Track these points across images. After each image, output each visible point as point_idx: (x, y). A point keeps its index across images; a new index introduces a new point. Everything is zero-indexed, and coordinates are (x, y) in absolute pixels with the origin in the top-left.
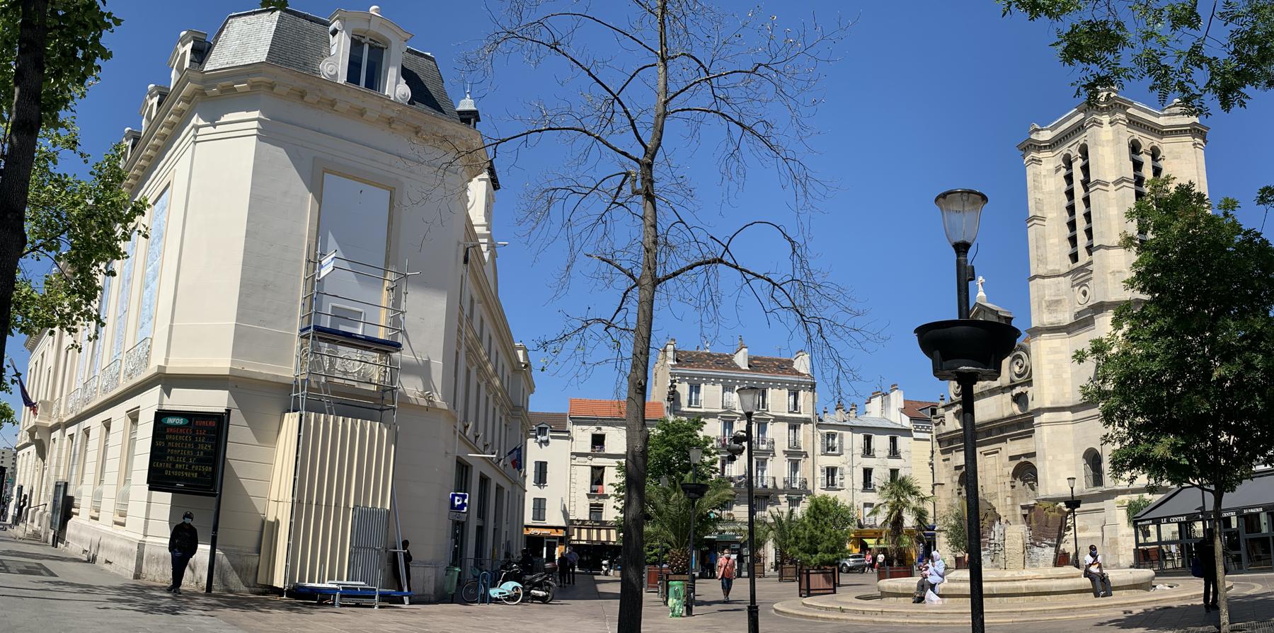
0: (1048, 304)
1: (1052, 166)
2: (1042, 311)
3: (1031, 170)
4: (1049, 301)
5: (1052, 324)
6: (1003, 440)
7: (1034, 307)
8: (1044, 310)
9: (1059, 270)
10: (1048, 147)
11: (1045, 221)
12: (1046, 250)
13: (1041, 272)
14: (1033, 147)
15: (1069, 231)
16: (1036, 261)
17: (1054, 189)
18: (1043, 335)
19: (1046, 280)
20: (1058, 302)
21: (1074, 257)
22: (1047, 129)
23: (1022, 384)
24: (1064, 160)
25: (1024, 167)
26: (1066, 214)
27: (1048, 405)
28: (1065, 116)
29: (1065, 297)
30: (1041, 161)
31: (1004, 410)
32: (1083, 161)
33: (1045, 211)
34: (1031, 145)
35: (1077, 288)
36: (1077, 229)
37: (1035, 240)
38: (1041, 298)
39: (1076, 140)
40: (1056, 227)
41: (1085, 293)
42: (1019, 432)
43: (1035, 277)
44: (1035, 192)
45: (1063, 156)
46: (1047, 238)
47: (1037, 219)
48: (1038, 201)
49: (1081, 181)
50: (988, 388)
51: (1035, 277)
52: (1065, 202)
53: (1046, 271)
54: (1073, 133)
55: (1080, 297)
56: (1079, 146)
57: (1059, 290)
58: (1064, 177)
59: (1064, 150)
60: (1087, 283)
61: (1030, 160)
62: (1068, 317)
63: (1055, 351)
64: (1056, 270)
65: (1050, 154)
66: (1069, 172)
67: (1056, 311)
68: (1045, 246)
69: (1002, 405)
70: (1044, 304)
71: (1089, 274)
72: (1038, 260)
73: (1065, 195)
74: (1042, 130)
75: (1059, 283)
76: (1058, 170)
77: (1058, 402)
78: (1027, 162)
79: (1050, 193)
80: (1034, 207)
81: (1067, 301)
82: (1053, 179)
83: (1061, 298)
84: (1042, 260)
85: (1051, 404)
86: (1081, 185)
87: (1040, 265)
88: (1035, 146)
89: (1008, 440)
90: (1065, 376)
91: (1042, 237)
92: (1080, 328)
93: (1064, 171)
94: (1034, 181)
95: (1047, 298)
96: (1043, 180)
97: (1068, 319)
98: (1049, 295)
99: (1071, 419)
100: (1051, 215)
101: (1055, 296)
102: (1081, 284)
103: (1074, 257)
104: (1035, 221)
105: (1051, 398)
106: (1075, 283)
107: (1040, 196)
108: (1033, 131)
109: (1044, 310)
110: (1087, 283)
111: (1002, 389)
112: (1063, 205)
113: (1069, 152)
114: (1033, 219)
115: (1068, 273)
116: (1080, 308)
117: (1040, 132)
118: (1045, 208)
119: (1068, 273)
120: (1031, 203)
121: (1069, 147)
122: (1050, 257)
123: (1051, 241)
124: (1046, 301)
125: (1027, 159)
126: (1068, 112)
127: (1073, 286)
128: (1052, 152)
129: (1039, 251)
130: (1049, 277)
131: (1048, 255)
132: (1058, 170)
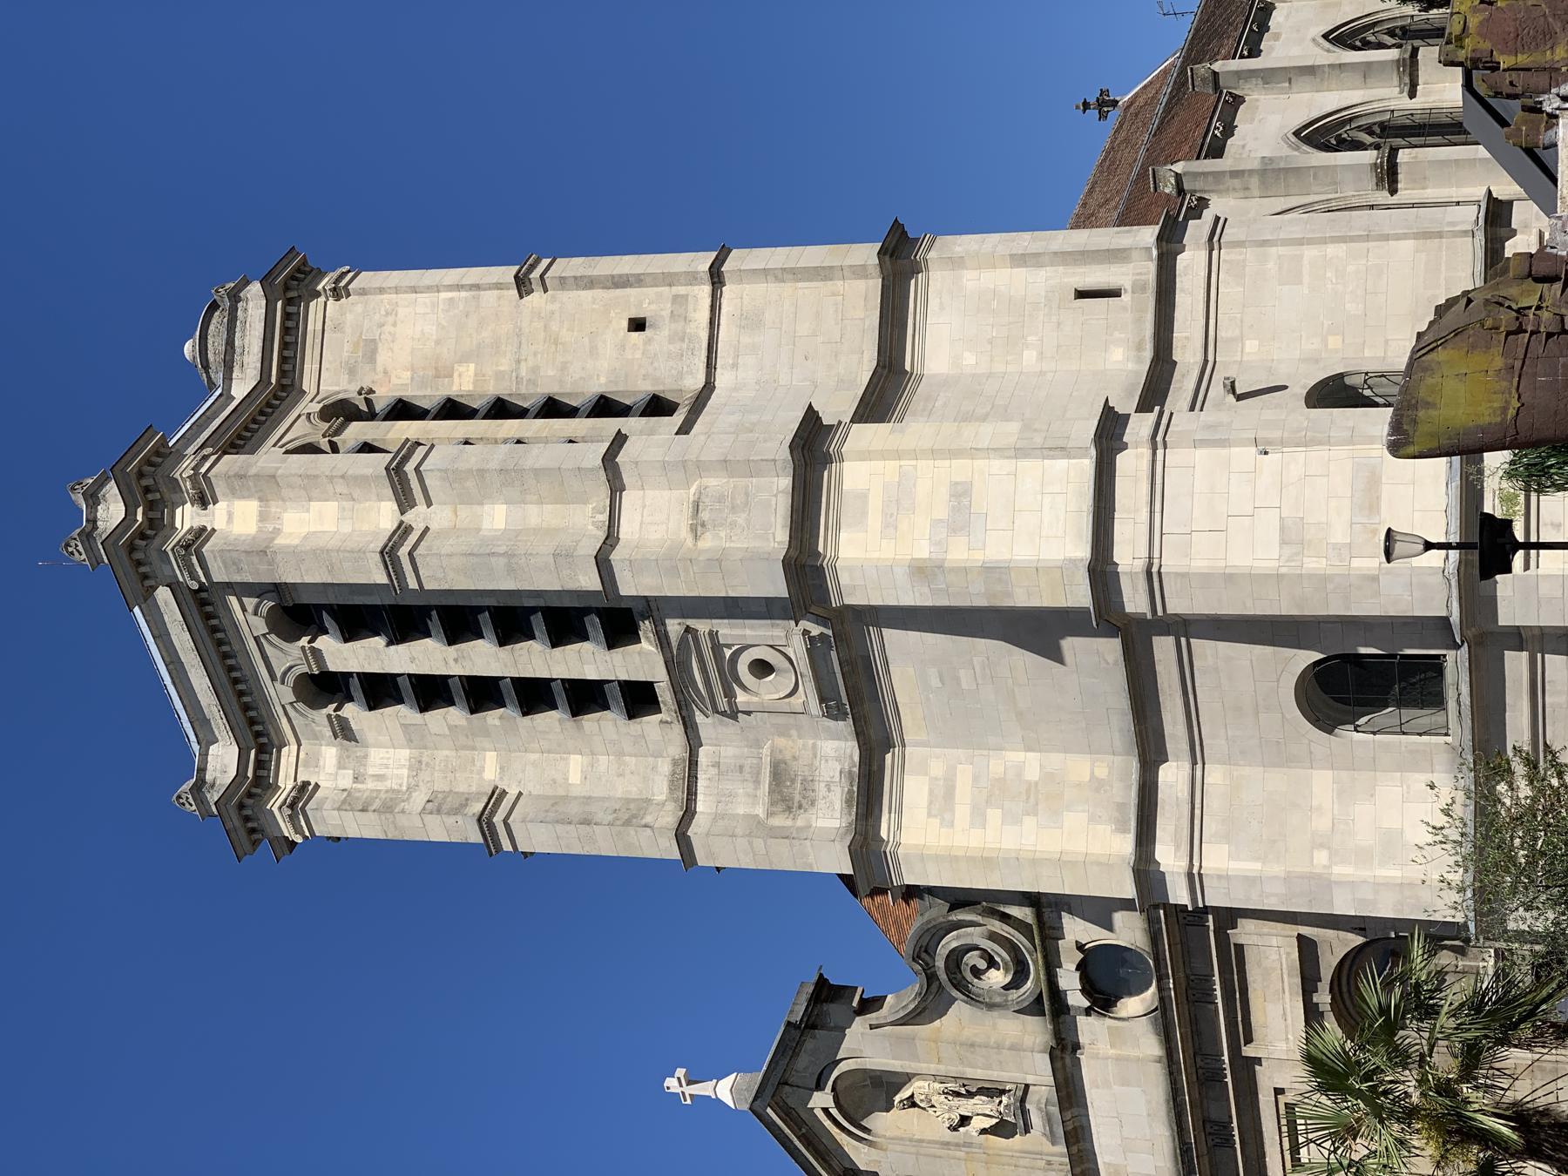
0: (780, 808)
1: (330, 753)
2: (799, 829)
3: (328, 820)
4: (773, 803)
5: (848, 802)
6: (1246, 1069)
7: (783, 858)
8: (800, 823)
9: (675, 763)
10: (265, 757)
11: (504, 793)
12: (603, 799)
13: (669, 817)
14: (250, 802)
15: (553, 713)
16: (632, 831)
17: (404, 754)
18: (884, 834)
19: (701, 807)
20: (779, 774)
21: (639, 699)
22: (204, 755)
23: (1051, 964)
24: (315, 704)
25: (313, 840)
26: (493, 717)
27: (1125, 845)
28: (168, 681)
29: (766, 751)
30: (306, 784)
31: (1134, 1053)
32: (326, 632)
33: (474, 789)
34: (241, 806)
35: (741, 698)
36: (545, 675)
37: (559, 827)
38: (757, 827)
39: (252, 645)
40: (534, 757)
41: (762, 668)
42: (1219, 1001)
43: (682, 838)
44: (403, 812)
45: (300, 706)
46: (561, 792)
47: (493, 813)
48: (435, 805)
49: (390, 643)
50: (1055, 1110)
51: (682, 838)
52: (455, 715)
53: (670, 806)
54: (225, 656)
55: (770, 690)
56: (273, 638)
57: (741, 768)
58: (371, 709)
59: (280, 695)
60: (728, 653)
61: (293, 819)
62: (836, 744)
63: (943, 800)
64: (674, 773)
65: (288, 756)
66: (355, 687)
67: (808, 784)
68: (588, 800)
69: (1118, 1059)
70: (779, 821)
71: (696, 639)
72: (627, 823)
73: (429, 715)
74: (202, 770)
75: (717, 765)
76: (344, 731)
77: (1121, 807)
78: (298, 830)
79: (417, 767)
80: (450, 820)
81: (781, 742)
82: (373, 752)
83: (767, 760)
84: (632, 814)
85: (1125, 831)
86: (402, 648)
87: (648, 819)
88: (250, 795)
89: (1248, 1051)
90: (1032, 773)
91: (557, 809)
92: (875, 697)
93: (353, 712)
94: (362, 810)
95: (760, 811)
96: (370, 785)
97: (842, 744)
98: (751, 802)
99: (1187, 765)
100: (489, 769)
101: (757, 782)
102: (730, 678)
103: (639, 699)
104: (498, 819)
105: (1105, 829)
106: (723, 703)
107: (419, 799)
108: (201, 801)
109: (800, 823)
110: (728, 653)
111: (1063, 1049)
112: (464, 722)
113: (291, 679)
114: (491, 826)
115: (690, 728)
116: (808, 695)
117: (209, 777)
118: (462, 788)
119: (690, 728)
120: (437, 831)
121: (273, 677)
122: (627, 787)
123: (575, 777)
124: (770, 814)
125: (287, 830)
126: (156, 672)
127: (733, 714)
128: (283, 744)
129: (600, 816)
130: (691, 794)
131: (619, 795)
132: (344, 731)
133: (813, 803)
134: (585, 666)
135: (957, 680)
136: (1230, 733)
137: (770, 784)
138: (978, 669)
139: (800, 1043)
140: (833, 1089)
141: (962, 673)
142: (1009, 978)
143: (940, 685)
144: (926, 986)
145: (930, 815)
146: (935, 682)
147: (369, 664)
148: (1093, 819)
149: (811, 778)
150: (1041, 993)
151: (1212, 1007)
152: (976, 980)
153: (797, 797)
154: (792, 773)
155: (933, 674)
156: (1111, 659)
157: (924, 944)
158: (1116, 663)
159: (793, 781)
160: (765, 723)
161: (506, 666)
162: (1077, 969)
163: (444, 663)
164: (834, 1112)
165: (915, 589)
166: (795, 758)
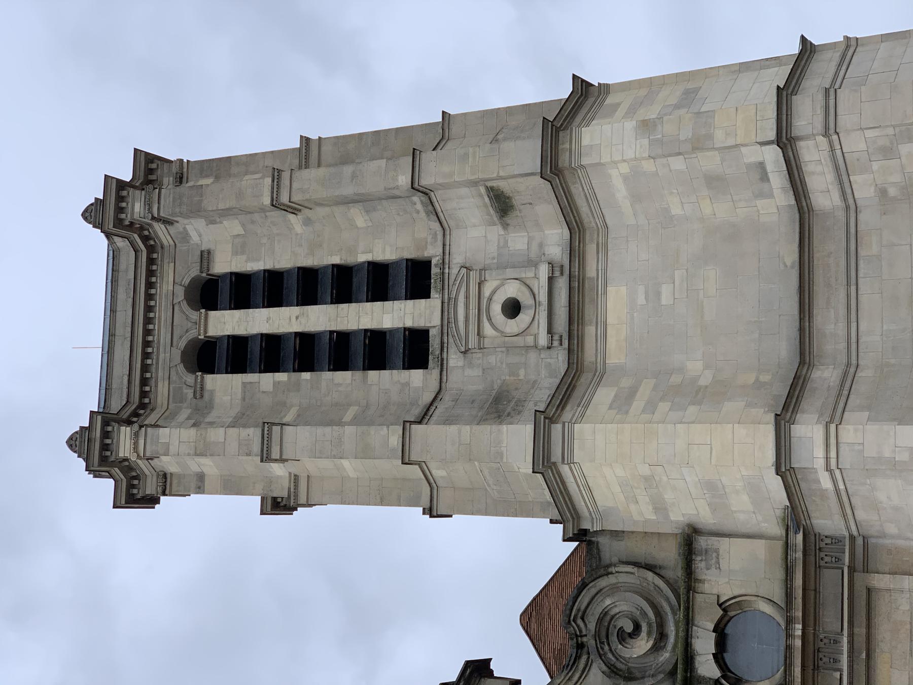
133: (520, 413)
134: (384, 315)
135: (658, 294)
136: (885, 327)
137: (491, 403)
138: (677, 283)
141: (664, 287)
142: (651, 643)
143: (644, 302)
144: (574, 655)
145: (610, 408)
146: (641, 300)
147: (239, 326)
148: (749, 405)
149: (525, 399)
150: (676, 663)
151: (837, 675)
152: (620, 646)
153: (509, 409)
154: (510, 397)
155: (641, 290)
156: (789, 263)
157: (583, 608)
158: (792, 267)
159: (509, 401)
160: (502, 363)
161: (329, 321)
162: (714, 631)
163: (288, 321)
165: (638, 141)
166: (516, 389)
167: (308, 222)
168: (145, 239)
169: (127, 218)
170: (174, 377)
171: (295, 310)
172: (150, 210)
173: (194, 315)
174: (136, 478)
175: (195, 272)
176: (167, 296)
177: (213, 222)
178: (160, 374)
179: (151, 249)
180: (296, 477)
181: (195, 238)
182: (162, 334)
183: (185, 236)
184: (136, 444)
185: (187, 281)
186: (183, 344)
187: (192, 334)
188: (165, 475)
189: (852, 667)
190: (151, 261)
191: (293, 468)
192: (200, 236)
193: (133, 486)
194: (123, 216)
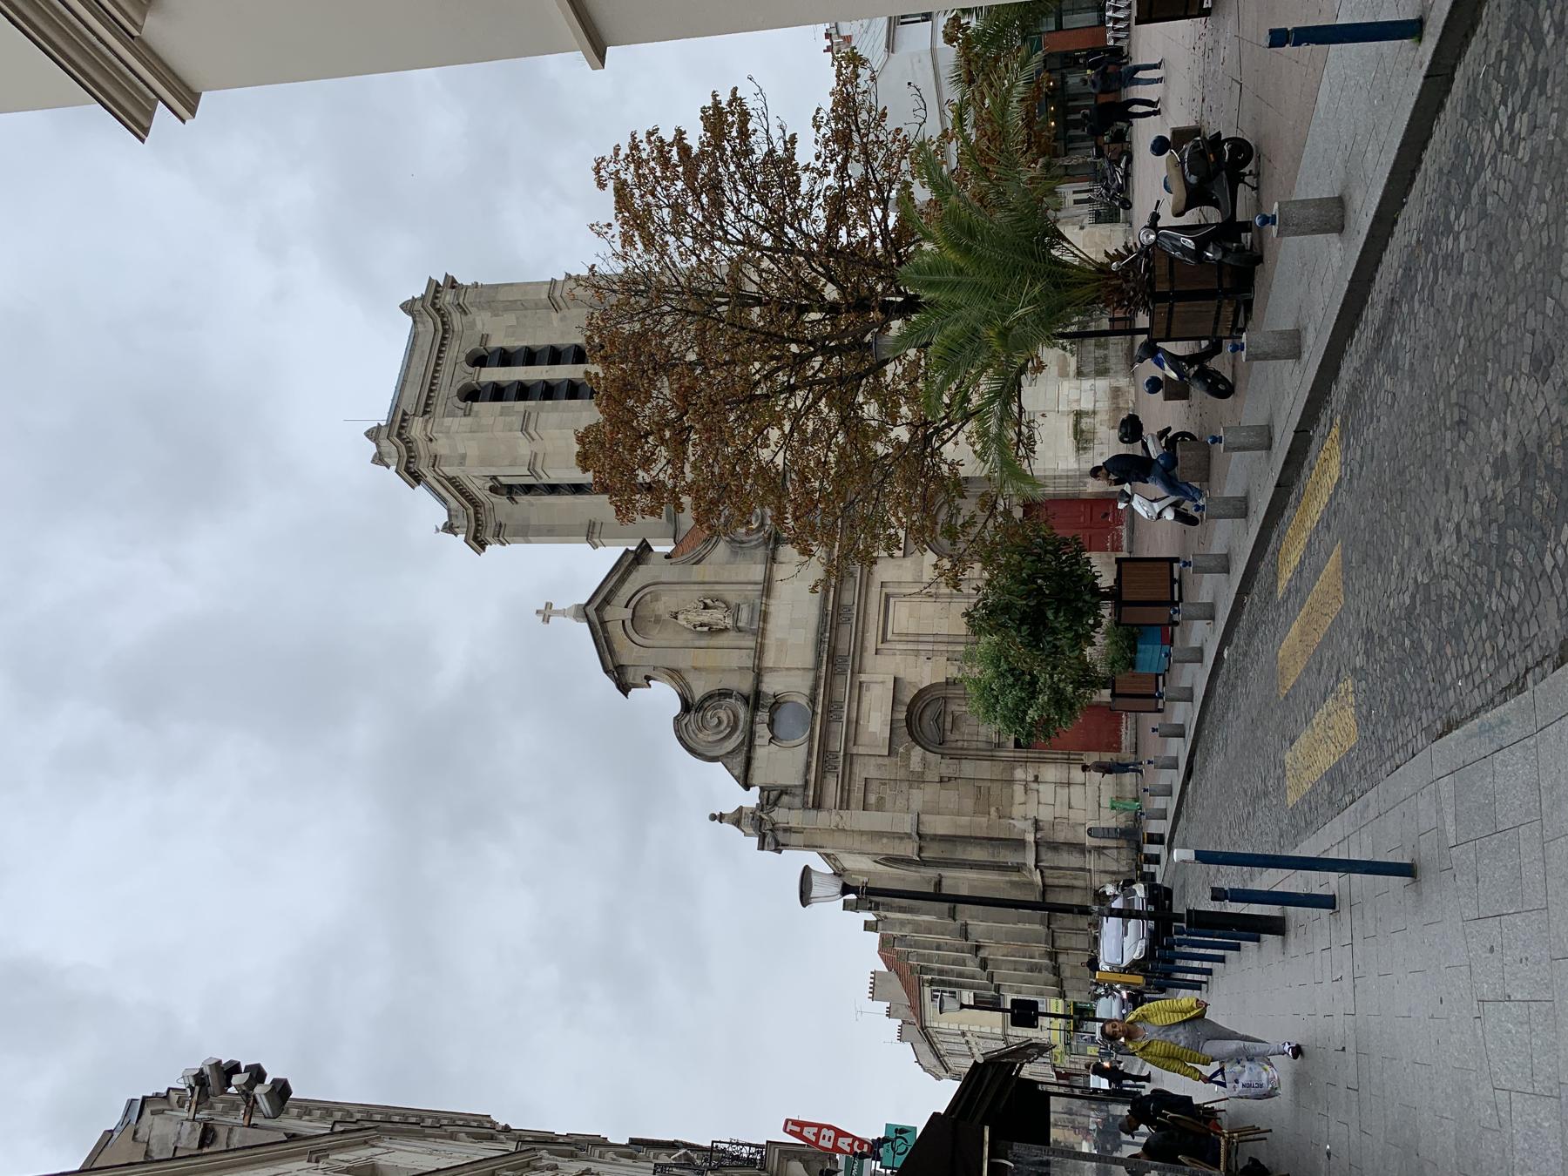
139: (628, 572)
140: (634, 609)
164: (628, 623)
167: (563, 319)
168: (444, 323)
169: (439, 304)
170: (449, 404)
171: (547, 367)
172: (458, 299)
173: (471, 370)
174: (412, 457)
175: (476, 346)
176: (451, 359)
177: (496, 315)
178: (439, 402)
179: (445, 331)
180: (536, 454)
181: (479, 326)
182: (444, 378)
183: (473, 324)
184: (425, 429)
185: (468, 351)
186: (459, 386)
187: (468, 380)
188: (436, 456)
189: (824, 751)
190: (443, 338)
191: (535, 447)
192: (483, 325)
193: (410, 462)
194: (437, 301)
